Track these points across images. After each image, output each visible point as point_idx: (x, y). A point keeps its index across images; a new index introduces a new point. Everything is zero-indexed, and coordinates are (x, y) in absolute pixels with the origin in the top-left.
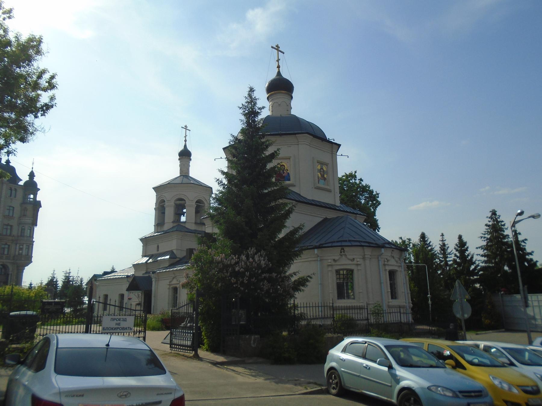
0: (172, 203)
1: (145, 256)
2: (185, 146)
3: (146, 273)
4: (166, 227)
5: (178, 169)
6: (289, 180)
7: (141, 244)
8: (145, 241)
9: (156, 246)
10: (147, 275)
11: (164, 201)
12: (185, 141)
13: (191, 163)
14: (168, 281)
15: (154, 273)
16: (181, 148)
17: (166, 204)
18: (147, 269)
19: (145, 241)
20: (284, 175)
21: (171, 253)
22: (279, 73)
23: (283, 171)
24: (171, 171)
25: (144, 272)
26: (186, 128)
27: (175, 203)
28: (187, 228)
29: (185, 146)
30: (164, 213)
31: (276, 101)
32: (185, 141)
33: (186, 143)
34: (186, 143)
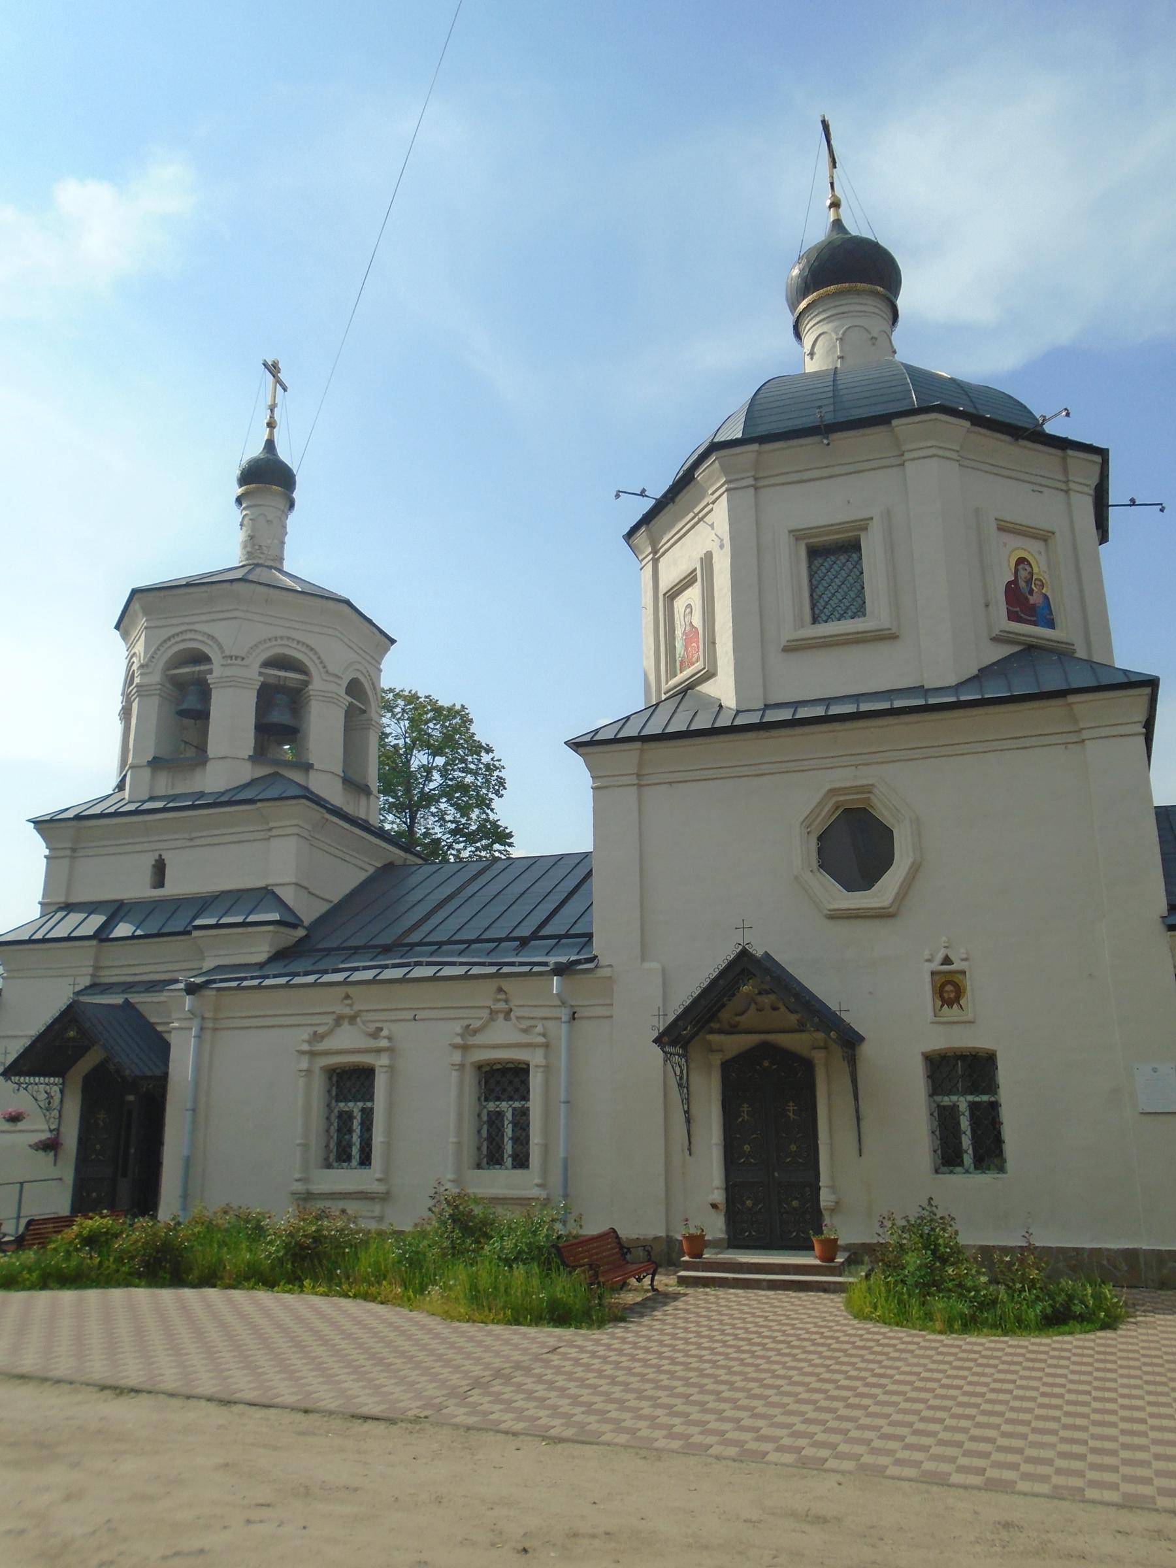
0: (253, 675)
1: (69, 908)
2: (270, 445)
3: (95, 987)
4: (215, 778)
5: (240, 536)
6: (1051, 624)
7: (37, 848)
8: (65, 832)
9: (149, 860)
10: (118, 1000)
11: (200, 658)
12: (271, 425)
13: (293, 521)
14: (305, 1034)
15: (192, 989)
16: (256, 450)
17: (217, 672)
18: (97, 968)
19: (65, 832)
20: (1032, 600)
21: (266, 895)
22: (838, 224)
23: (1029, 581)
24: (210, 539)
25: (86, 981)
26: (273, 369)
27: (260, 674)
28: (312, 793)
29: (270, 445)
30: (201, 716)
31: (858, 322)
32: (271, 425)
33: (271, 434)
34: (271, 434)
